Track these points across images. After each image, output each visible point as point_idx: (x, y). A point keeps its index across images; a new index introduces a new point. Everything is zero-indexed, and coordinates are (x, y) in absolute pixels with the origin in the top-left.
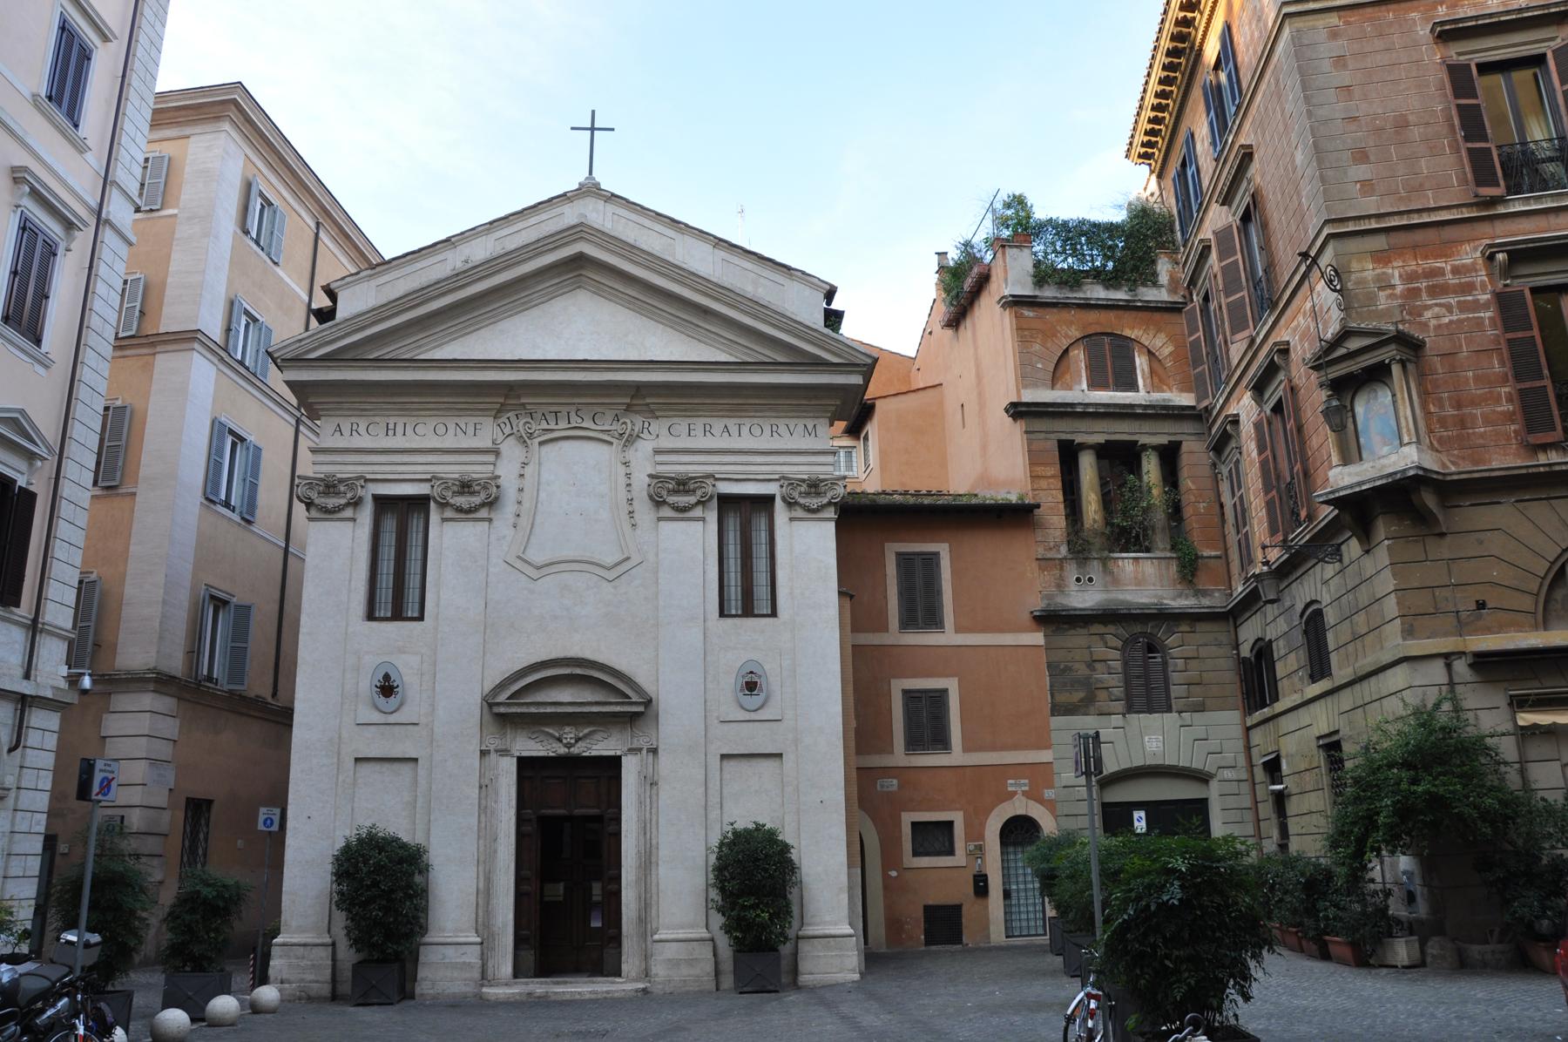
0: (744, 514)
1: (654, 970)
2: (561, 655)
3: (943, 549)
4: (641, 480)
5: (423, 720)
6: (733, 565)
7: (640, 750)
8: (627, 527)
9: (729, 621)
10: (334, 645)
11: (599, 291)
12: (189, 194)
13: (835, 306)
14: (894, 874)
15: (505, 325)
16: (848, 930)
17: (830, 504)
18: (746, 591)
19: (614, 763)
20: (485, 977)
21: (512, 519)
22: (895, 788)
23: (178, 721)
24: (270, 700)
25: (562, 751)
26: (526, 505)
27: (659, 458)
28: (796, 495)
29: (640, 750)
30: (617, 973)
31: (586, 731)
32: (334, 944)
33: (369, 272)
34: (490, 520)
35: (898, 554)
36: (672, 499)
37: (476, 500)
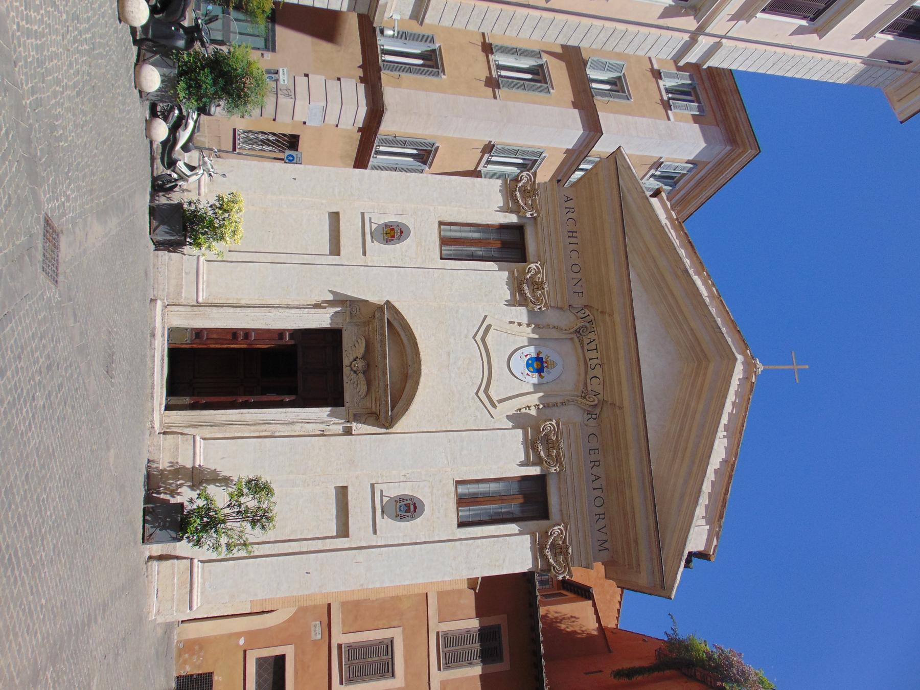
5: (369, 259)
9: (453, 489)
14: (242, 642)
22: (313, 637)
35: (499, 627)
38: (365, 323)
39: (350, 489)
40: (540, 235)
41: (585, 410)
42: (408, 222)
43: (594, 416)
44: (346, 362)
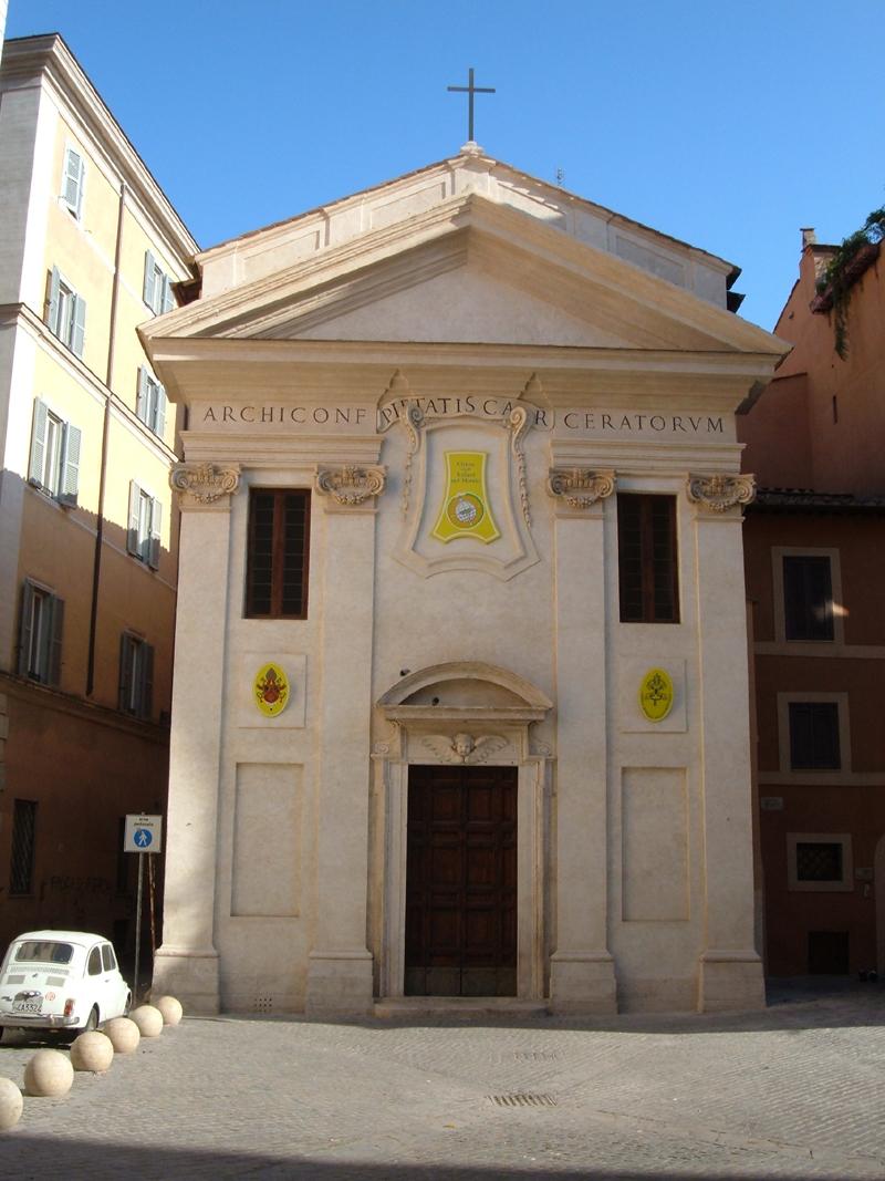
3: (834, 555)
4: (540, 473)
13: (735, 289)
16: (758, 957)
17: (737, 504)
23: (7, 720)
24: (85, 698)
32: (219, 957)
35: (786, 559)
38: (402, 734)
40: (267, 465)
41: (532, 427)
44: (456, 760)
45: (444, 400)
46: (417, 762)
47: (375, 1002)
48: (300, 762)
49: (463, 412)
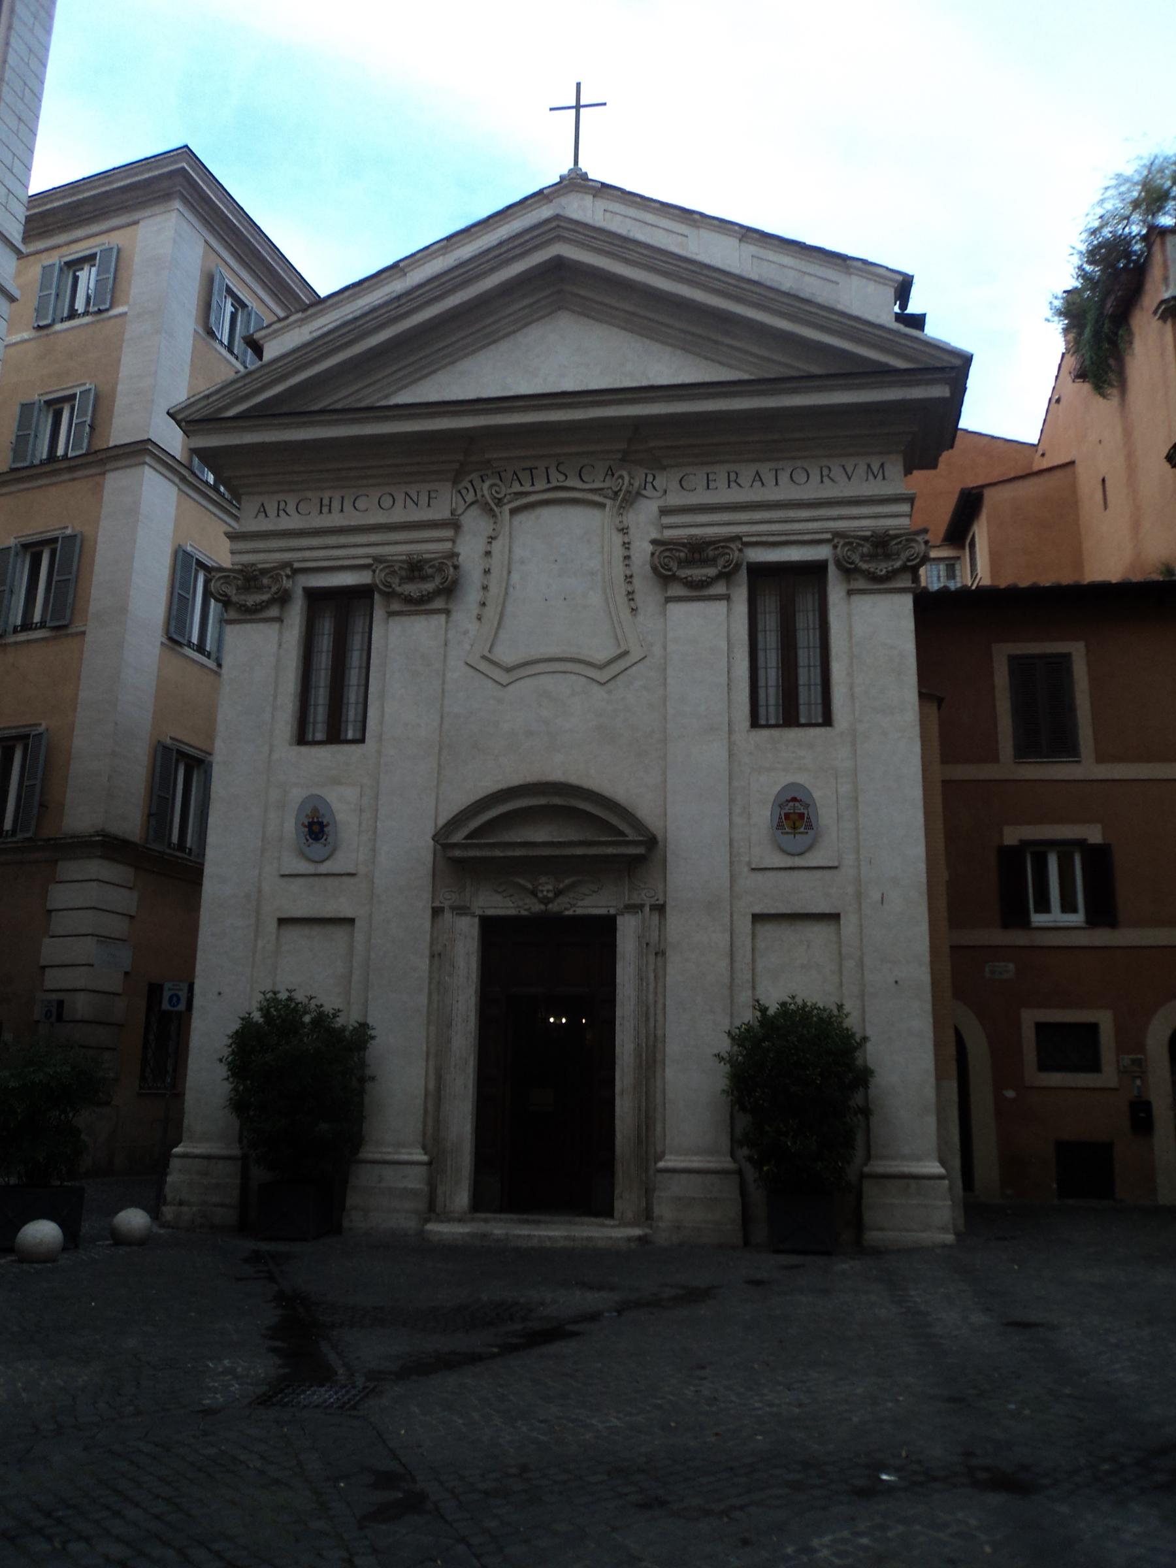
0: (787, 600)
1: (657, 1211)
2: (530, 779)
3: (1077, 651)
4: (642, 549)
6: (771, 660)
7: (641, 907)
8: (625, 614)
9: (765, 733)
10: (258, 775)
11: (588, 311)
12: (140, 287)
14: (1010, 1094)
15: (466, 364)
18: (790, 689)
19: (606, 927)
20: (433, 1209)
21: (475, 609)
25: (538, 908)
26: (494, 590)
27: (666, 520)
28: (856, 558)
29: (641, 907)
30: (609, 1212)
31: (567, 882)
33: (300, 315)
34: (447, 612)
35: (1012, 659)
36: (684, 573)
37: (429, 586)
39: (757, 910)
41: (638, 494)
42: (297, 795)
43: (650, 478)
45: (531, 470)
46: (490, 912)
47: (427, 1221)
48: (349, 915)
49: (554, 484)
